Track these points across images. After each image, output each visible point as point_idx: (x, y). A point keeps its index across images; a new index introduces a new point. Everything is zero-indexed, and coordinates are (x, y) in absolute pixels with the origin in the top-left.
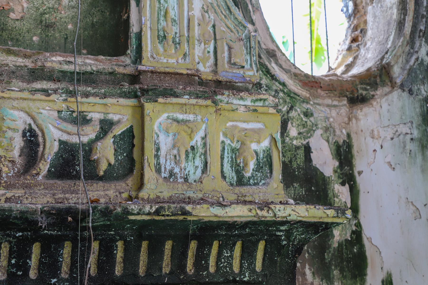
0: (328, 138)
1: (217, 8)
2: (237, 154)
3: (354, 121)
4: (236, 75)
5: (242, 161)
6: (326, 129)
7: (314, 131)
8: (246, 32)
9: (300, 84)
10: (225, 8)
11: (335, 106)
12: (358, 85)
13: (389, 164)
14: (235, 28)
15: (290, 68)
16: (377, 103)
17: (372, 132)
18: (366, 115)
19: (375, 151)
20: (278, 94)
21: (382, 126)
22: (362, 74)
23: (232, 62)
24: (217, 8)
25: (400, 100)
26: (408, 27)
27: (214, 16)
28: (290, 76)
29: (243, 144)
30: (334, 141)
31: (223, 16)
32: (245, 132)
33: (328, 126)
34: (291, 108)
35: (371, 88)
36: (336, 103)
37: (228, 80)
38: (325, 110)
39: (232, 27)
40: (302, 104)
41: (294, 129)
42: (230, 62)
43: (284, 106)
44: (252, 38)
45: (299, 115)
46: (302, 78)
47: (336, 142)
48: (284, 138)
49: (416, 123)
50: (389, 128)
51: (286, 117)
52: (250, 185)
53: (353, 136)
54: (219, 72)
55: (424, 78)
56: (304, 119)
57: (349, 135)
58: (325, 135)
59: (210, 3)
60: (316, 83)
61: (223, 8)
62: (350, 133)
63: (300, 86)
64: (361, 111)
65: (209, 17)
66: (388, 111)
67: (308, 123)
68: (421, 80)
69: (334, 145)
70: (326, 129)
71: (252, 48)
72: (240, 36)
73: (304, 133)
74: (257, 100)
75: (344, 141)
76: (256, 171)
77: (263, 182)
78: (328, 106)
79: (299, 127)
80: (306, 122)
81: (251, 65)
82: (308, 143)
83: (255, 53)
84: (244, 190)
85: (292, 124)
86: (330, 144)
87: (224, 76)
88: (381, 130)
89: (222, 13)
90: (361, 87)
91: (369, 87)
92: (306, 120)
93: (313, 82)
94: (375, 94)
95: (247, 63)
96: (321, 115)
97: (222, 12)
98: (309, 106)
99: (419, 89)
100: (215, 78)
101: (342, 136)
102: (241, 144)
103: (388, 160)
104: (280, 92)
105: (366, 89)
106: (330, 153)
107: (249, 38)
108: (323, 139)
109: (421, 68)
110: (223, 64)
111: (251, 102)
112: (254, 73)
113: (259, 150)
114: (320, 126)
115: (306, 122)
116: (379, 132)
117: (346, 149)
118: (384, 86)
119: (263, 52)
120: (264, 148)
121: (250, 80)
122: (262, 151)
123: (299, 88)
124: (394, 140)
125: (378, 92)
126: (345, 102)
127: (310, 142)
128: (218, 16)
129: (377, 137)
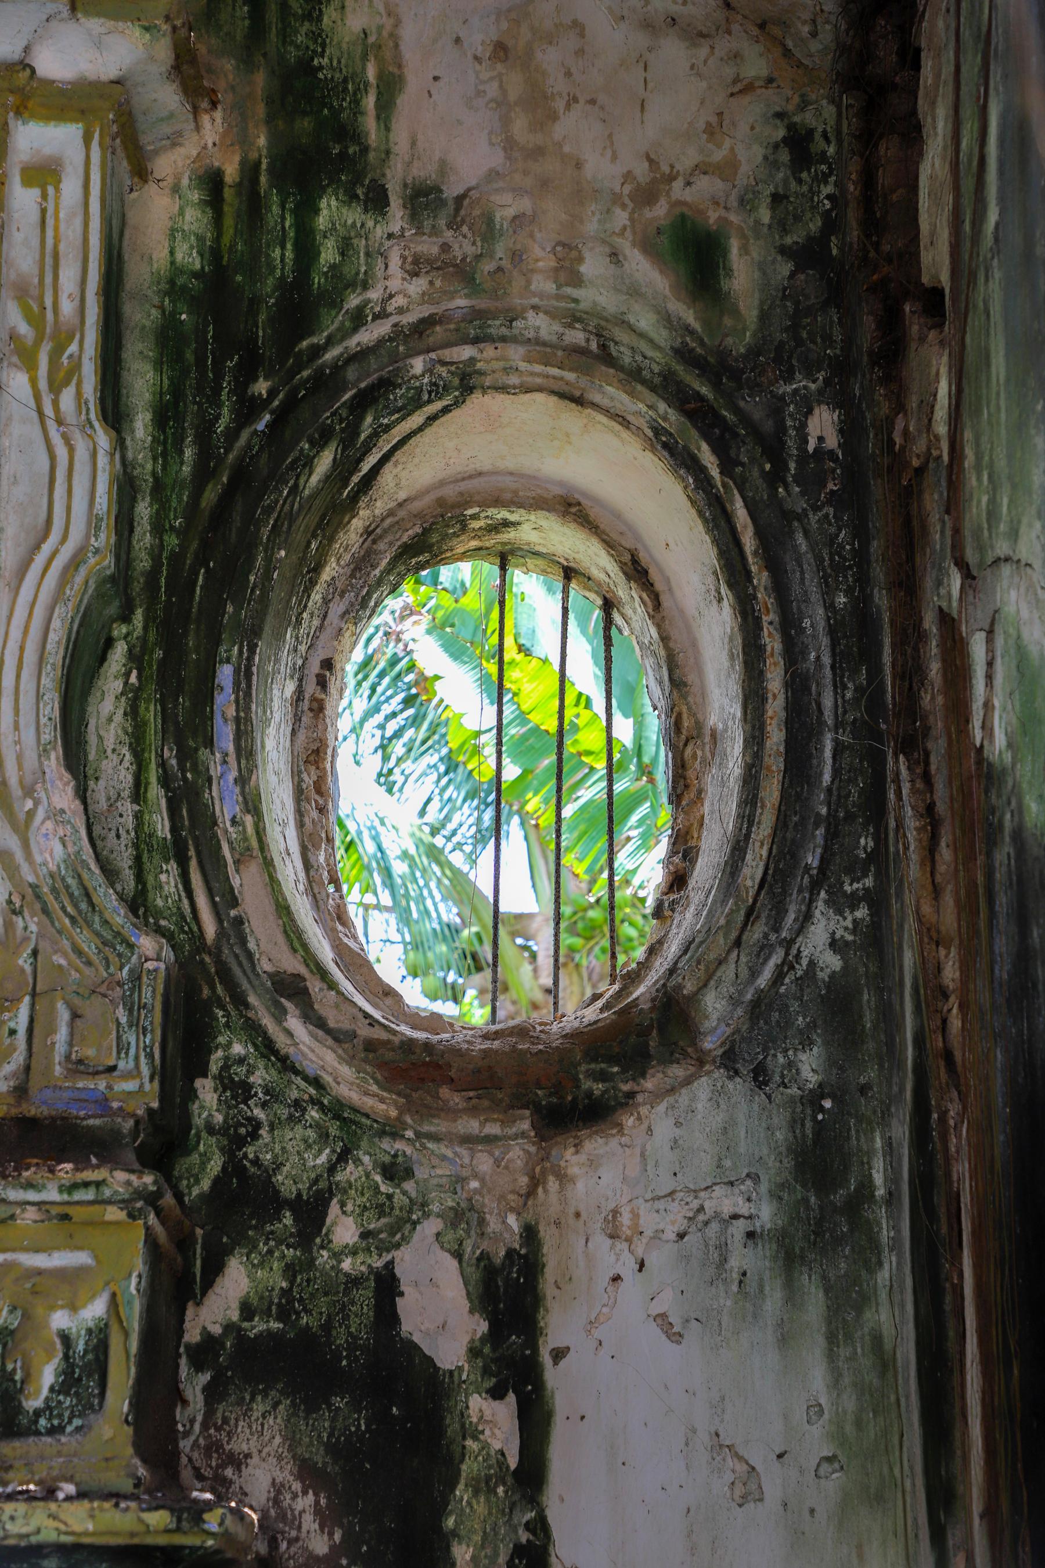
0: (461, 1244)
1: (50, 899)
2: (10, 1344)
3: (552, 1184)
4: (83, 1096)
5: (19, 1364)
6: (456, 1217)
7: (415, 1224)
8: (135, 957)
9: (379, 1076)
10: (76, 893)
11: (489, 1140)
12: (580, 1064)
13: (662, 1318)
14: (100, 951)
15: (353, 1026)
16: (639, 1118)
17: (614, 1217)
18: (593, 1163)
19: (616, 1278)
20: (303, 1115)
21: (649, 1196)
22: (600, 1024)
23: (74, 1056)
24: (50, 899)
25: (718, 1106)
26: (754, 864)
27: (38, 924)
28: (351, 1053)
29: (26, 1316)
30: (478, 1252)
31: (67, 921)
32: (33, 1280)
33: (463, 1205)
34: (343, 1157)
35: (624, 1071)
36: (493, 1129)
37: (54, 1113)
38: (455, 1153)
39: (90, 948)
40: (376, 1140)
41: (350, 1221)
42: (68, 1057)
43: (320, 1152)
44: (145, 979)
45: (368, 1175)
46: (389, 1055)
47: (484, 1256)
48: (311, 1252)
49: (770, 1181)
50: (673, 1200)
51: (322, 1185)
52: (38, 1433)
53: (547, 1234)
54: (30, 1092)
55: (812, 1026)
56: (383, 1188)
57: (530, 1233)
58: (450, 1236)
59: (30, 885)
60: (438, 1066)
61: (71, 895)
62: (537, 1224)
63: (377, 1082)
64: (577, 1152)
65: (26, 928)
66: (675, 1144)
67: (395, 1200)
68: (801, 1032)
69: (478, 1266)
70: (456, 1217)
71: (144, 1007)
72: (111, 975)
73: (381, 1231)
74: (74, 1187)
75: (510, 1253)
76: (59, 1393)
77: (77, 1422)
78: (468, 1140)
79: (366, 1214)
80: (390, 1197)
81: (137, 1058)
82: (390, 1265)
83: (152, 1023)
84: (14, 1449)
85: (343, 1205)
86: (464, 1265)
87: (44, 1103)
88: (643, 1208)
89: (65, 911)
90: (587, 1071)
91: (616, 1069)
92: (391, 1191)
93: (425, 1064)
94: (636, 1088)
95: (127, 1054)
96: (439, 1172)
97: (63, 909)
98: (399, 1145)
99: (790, 1064)
100: (14, 1111)
101: (506, 1235)
102: (23, 1316)
103: (656, 1308)
104: (309, 1108)
105: (603, 1077)
106: (464, 1292)
107: (139, 978)
108: (442, 1247)
109: (807, 991)
110: (49, 1067)
111: (61, 1191)
112: (142, 1086)
113: (74, 1330)
114: (435, 1207)
115: (390, 1197)
116: (635, 1216)
117: (518, 1278)
118: (672, 1062)
119: (263, 984)
120: (91, 1324)
121: (120, 1109)
122: (83, 1332)
123: (374, 1088)
124: (686, 1239)
125: (649, 1084)
126: (525, 1125)
127: (396, 1261)
128: (53, 923)
129: (629, 1233)
